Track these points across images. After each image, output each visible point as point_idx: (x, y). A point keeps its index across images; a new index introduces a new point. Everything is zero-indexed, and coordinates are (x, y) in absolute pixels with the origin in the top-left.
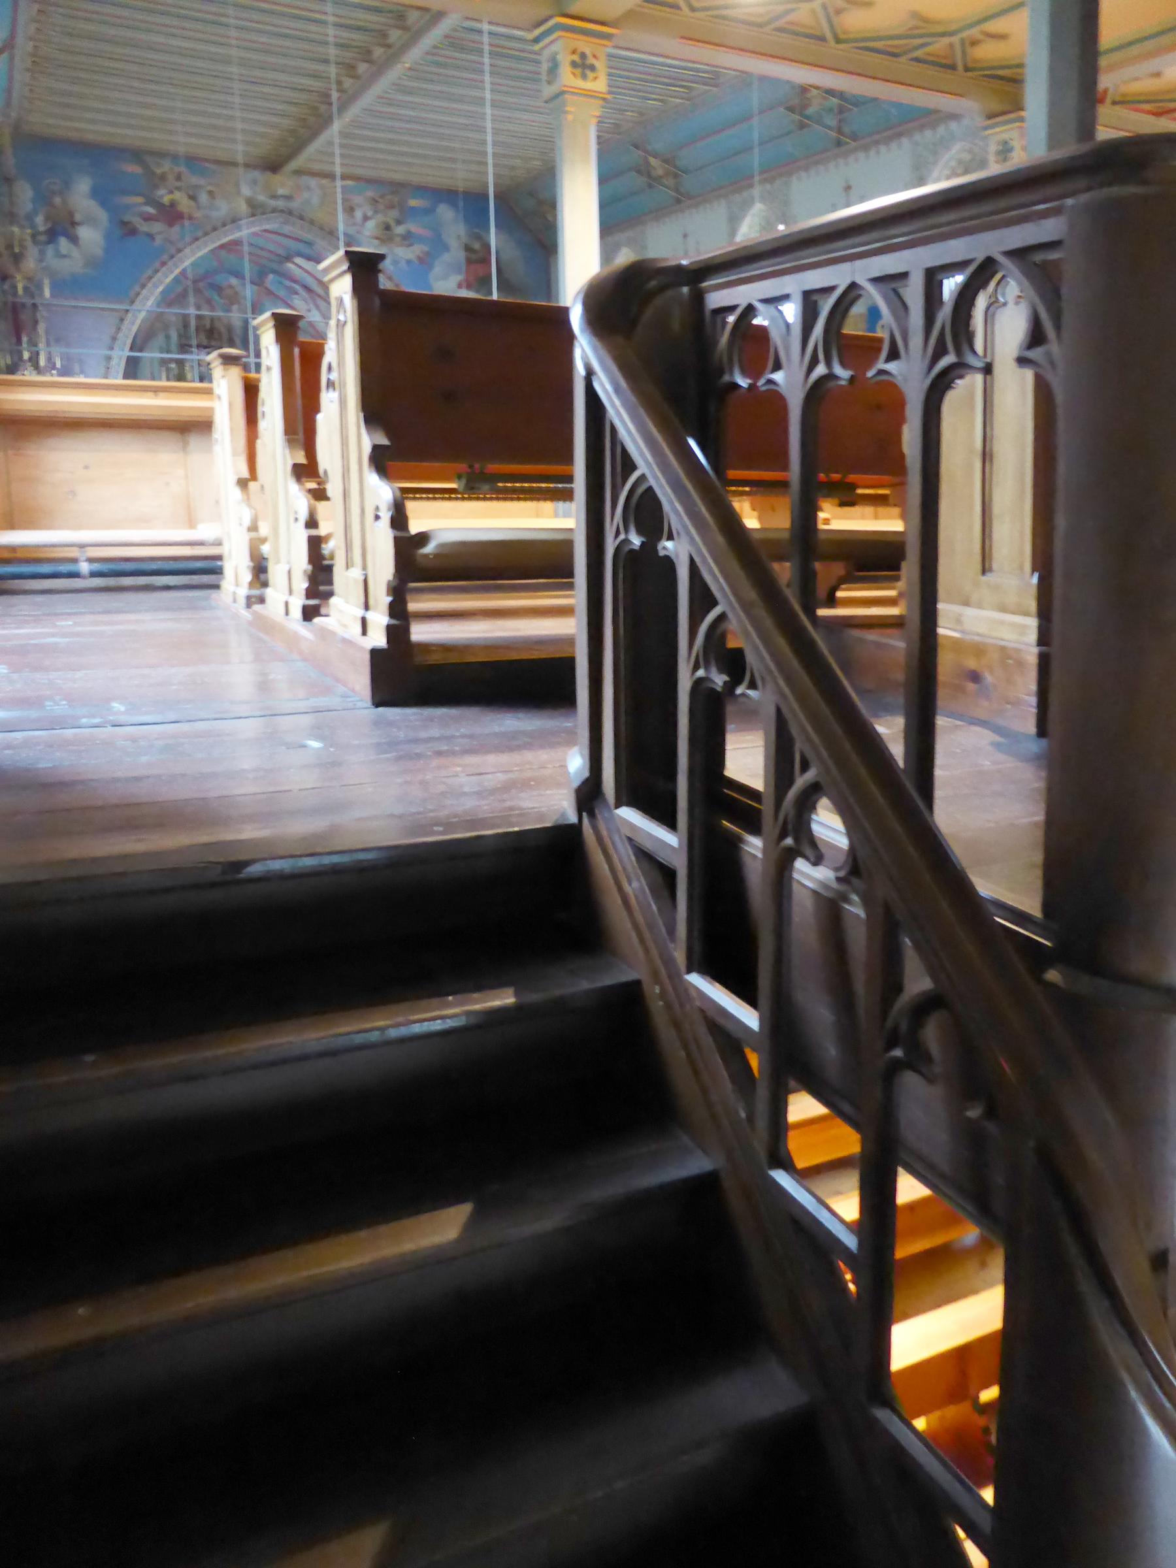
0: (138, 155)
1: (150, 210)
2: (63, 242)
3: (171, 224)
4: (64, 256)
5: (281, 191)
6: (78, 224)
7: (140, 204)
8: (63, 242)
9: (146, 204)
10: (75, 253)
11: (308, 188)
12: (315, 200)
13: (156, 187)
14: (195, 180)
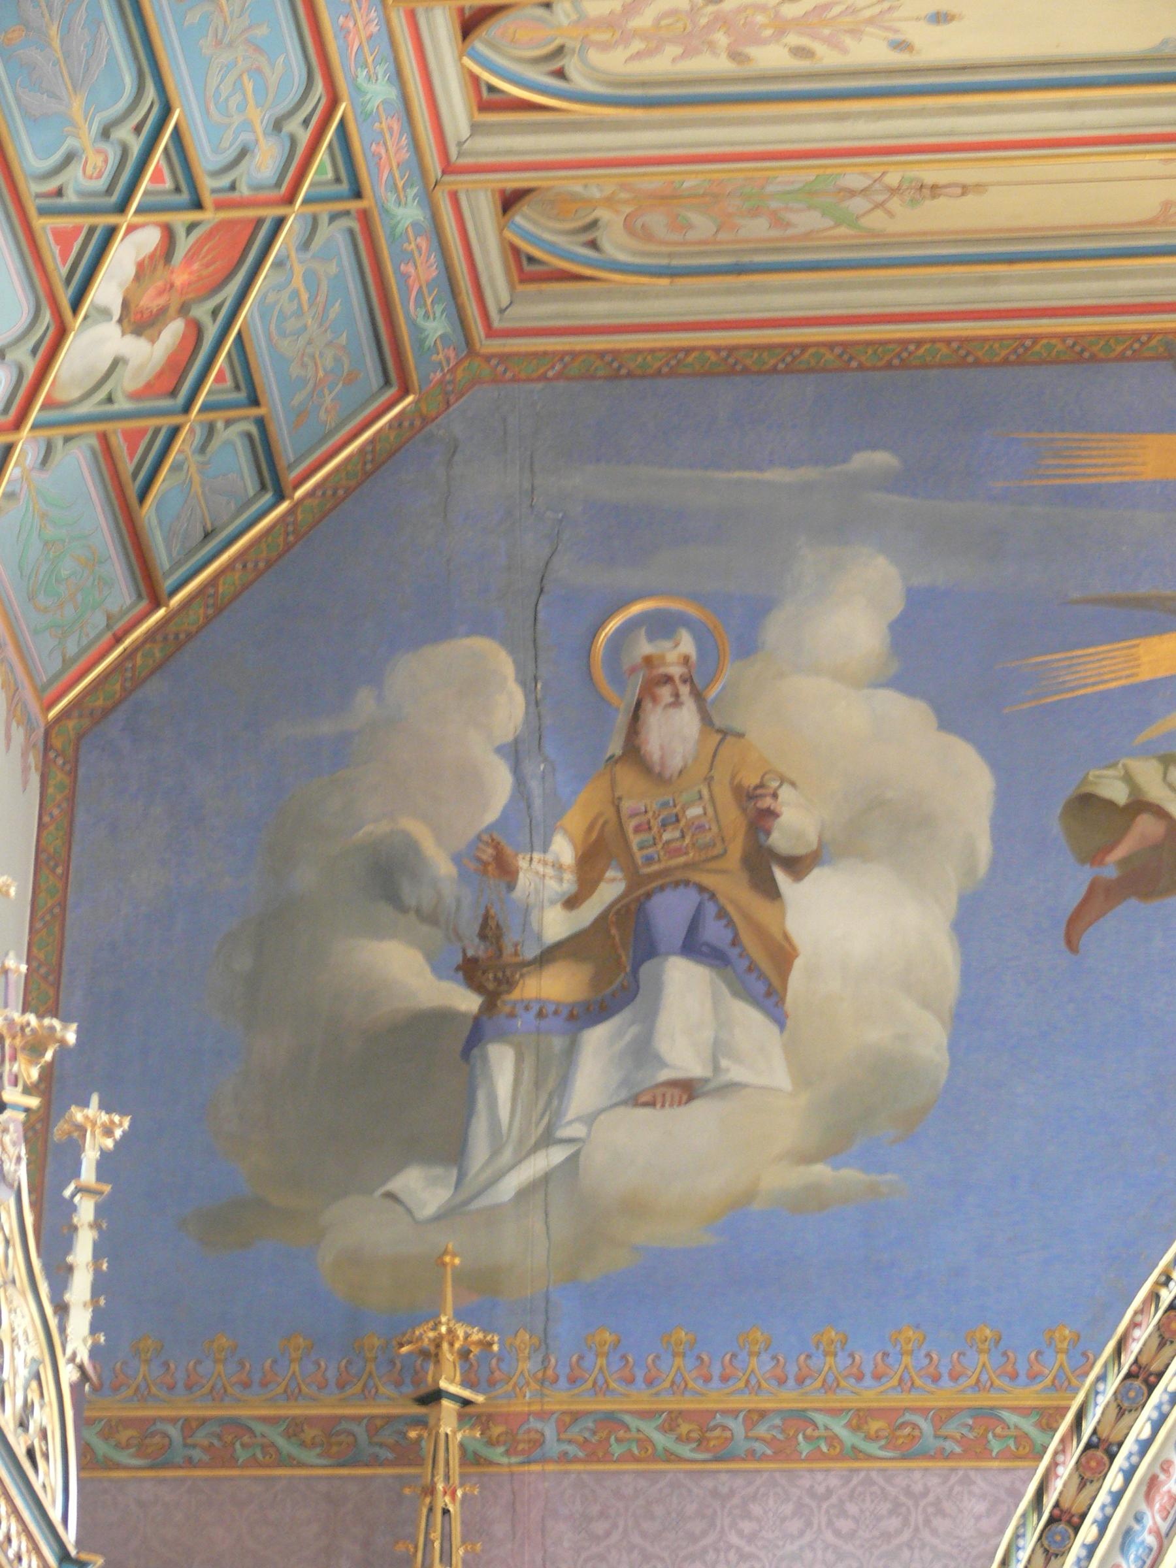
6: (797, 866)
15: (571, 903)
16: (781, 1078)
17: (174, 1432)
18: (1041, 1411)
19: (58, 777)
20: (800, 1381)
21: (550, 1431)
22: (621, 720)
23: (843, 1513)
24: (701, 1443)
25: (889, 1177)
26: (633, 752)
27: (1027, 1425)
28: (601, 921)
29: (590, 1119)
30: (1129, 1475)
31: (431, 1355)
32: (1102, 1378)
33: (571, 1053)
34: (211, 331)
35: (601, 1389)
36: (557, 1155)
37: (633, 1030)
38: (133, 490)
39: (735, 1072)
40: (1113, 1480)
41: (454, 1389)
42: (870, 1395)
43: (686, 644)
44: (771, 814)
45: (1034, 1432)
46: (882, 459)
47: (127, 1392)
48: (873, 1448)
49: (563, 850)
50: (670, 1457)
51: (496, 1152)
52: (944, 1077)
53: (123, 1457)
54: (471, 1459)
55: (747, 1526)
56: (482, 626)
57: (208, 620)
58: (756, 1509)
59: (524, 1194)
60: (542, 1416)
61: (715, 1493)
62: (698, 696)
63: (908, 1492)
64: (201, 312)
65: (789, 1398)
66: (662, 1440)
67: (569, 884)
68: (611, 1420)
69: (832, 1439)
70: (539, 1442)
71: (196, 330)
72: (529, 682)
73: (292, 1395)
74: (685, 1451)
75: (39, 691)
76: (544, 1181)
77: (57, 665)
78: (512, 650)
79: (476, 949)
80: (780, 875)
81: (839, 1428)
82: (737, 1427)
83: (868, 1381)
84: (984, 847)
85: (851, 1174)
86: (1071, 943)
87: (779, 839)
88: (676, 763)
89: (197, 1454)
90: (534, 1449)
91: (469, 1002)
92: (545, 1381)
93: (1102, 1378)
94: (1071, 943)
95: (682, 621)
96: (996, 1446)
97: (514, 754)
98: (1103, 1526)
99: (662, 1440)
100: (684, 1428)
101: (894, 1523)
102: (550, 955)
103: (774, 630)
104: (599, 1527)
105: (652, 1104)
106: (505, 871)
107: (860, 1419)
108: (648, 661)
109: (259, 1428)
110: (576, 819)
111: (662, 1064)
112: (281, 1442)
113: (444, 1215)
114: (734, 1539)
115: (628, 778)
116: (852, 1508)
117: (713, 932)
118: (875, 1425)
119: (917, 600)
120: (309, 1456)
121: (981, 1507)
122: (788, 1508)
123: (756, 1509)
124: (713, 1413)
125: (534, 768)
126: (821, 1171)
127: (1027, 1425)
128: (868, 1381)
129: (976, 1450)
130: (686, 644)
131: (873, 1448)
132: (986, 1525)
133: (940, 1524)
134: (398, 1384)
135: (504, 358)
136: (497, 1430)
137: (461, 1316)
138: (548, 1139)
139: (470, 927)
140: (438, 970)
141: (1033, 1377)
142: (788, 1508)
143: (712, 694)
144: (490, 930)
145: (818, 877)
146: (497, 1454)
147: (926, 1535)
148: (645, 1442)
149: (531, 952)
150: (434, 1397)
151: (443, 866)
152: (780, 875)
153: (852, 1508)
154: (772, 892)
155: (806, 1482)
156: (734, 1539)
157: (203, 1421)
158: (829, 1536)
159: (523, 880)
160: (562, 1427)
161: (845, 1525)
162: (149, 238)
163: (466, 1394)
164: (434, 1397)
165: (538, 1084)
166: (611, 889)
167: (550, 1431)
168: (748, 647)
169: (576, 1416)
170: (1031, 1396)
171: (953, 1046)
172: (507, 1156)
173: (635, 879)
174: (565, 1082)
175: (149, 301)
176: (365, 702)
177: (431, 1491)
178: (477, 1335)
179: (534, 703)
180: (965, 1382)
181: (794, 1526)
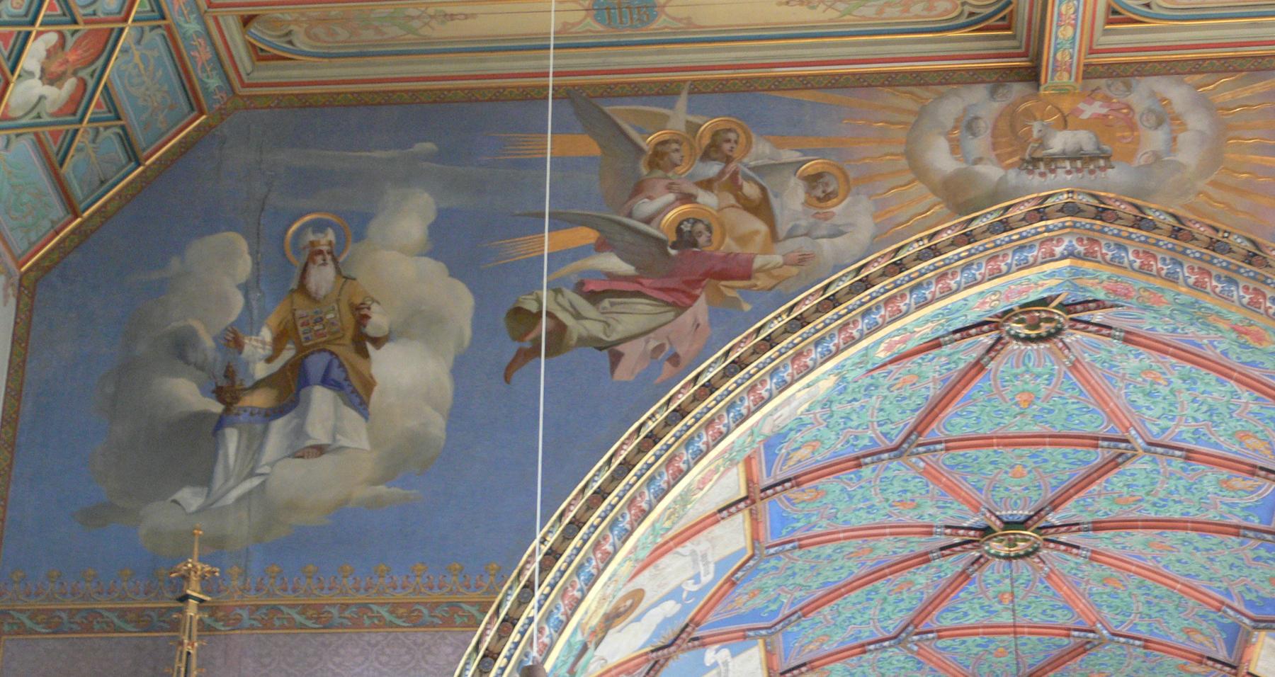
1: (613, 263)
2: (321, 400)
3: (679, 299)
4: (320, 450)
5: (1060, 141)
6: (378, 342)
7: (580, 253)
8: (321, 400)
9: (602, 246)
10: (356, 434)
11: (1164, 117)
12: (1189, 155)
13: (638, 189)
14: (762, 150)
15: (269, 360)
16: (365, 445)
17: (64, 615)
18: (480, 603)
19: (25, 299)
20: (366, 590)
21: (245, 614)
22: (298, 272)
23: (383, 654)
24: (318, 619)
25: (414, 491)
26: (302, 288)
27: (474, 610)
28: (283, 370)
29: (272, 464)
30: (523, 634)
31: (185, 578)
32: (510, 588)
33: (265, 431)
34: (91, 83)
35: (271, 594)
36: (255, 482)
37: (295, 422)
38: (55, 160)
39: (343, 441)
40: (515, 636)
41: (195, 594)
42: (400, 596)
43: (331, 235)
44: (367, 317)
45: (477, 614)
46: (429, 146)
47: (43, 597)
48: (399, 622)
49: (267, 334)
50: (303, 627)
51: (226, 480)
52: (442, 443)
53: (39, 629)
54: (204, 627)
55: (337, 660)
56: (232, 227)
57: (102, 223)
58: (342, 651)
59: (240, 500)
60: (241, 607)
61: (323, 644)
62: (335, 260)
63: (415, 644)
64: (84, 74)
65: (361, 598)
66: (299, 618)
67: (268, 351)
68: (275, 609)
69: (381, 618)
70: (239, 620)
71: (83, 83)
72: (254, 253)
73: (123, 598)
74: (309, 623)
75: (15, 258)
76: (249, 493)
77: (25, 245)
78: (247, 238)
79: (223, 382)
80: (370, 347)
81: (384, 612)
82: (335, 611)
83: (399, 590)
84: (468, 333)
85: (396, 491)
86: (507, 378)
87: (370, 330)
88: (322, 292)
89: (74, 626)
90: (237, 623)
91: (218, 408)
92: (244, 590)
93: (510, 588)
94: (507, 378)
95: (328, 224)
96: (458, 621)
97: (245, 288)
98: (509, 658)
99: (299, 618)
100: (310, 613)
101: (407, 658)
102: (257, 385)
103: (373, 228)
104: (267, 661)
105: (302, 457)
106: (238, 345)
107: (393, 608)
108: (312, 243)
109: (106, 614)
110: (273, 320)
111: (308, 437)
112: (116, 620)
113: (200, 510)
114: (331, 666)
115: (299, 300)
116: (388, 651)
117: (336, 374)
118: (310, 613)
119: (441, 214)
120: (129, 627)
121: (449, 650)
122: (404, 650)
123: (342, 651)
124: (323, 605)
125: (255, 295)
126: (382, 489)
127: (474, 610)
128: (399, 590)
129: (448, 622)
130: (331, 235)
131: (399, 622)
132: (451, 658)
133: (430, 658)
134: (173, 592)
135: (249, 97)
136: (220, 614)
137: (200, 560)
138: (252, 474)
139: (219, 370)
140: (204, 392)
141: (478, 587)
142: (357, 651)
143: (341, 260)
144: (229, 373)
145: (388, 348)
146: (219, 625)
147: (423, 664)
148: (291, 620)
149: (248, 384)
150: (185, 598)
151: (208, 342)
152: (370, 347)
153: (388, 651)
154: (365, 354)
155: (366, 638)
156: (331, 666)
157: (79, 610)
158: (376, 664)
159: (247, 349)
160: (252, 612)
161: (384, 659)
162: (51, 38)
163: (201, 596)
164: (185, 598)
165: (248, 447)
166: (288, 353)
167: (245, 614)
168: (360, 237)
169: (258, 607)
170: (476, 596)
171: (448, 428)
172: (231, 482)
173: (300, 348)
174: (261, 446)
175: (55, 68)
176: (175, 263)
177: (181, 643)
178: (207, 568)
179: (256, 264)
180: (445, 590)
181: (361, 659)
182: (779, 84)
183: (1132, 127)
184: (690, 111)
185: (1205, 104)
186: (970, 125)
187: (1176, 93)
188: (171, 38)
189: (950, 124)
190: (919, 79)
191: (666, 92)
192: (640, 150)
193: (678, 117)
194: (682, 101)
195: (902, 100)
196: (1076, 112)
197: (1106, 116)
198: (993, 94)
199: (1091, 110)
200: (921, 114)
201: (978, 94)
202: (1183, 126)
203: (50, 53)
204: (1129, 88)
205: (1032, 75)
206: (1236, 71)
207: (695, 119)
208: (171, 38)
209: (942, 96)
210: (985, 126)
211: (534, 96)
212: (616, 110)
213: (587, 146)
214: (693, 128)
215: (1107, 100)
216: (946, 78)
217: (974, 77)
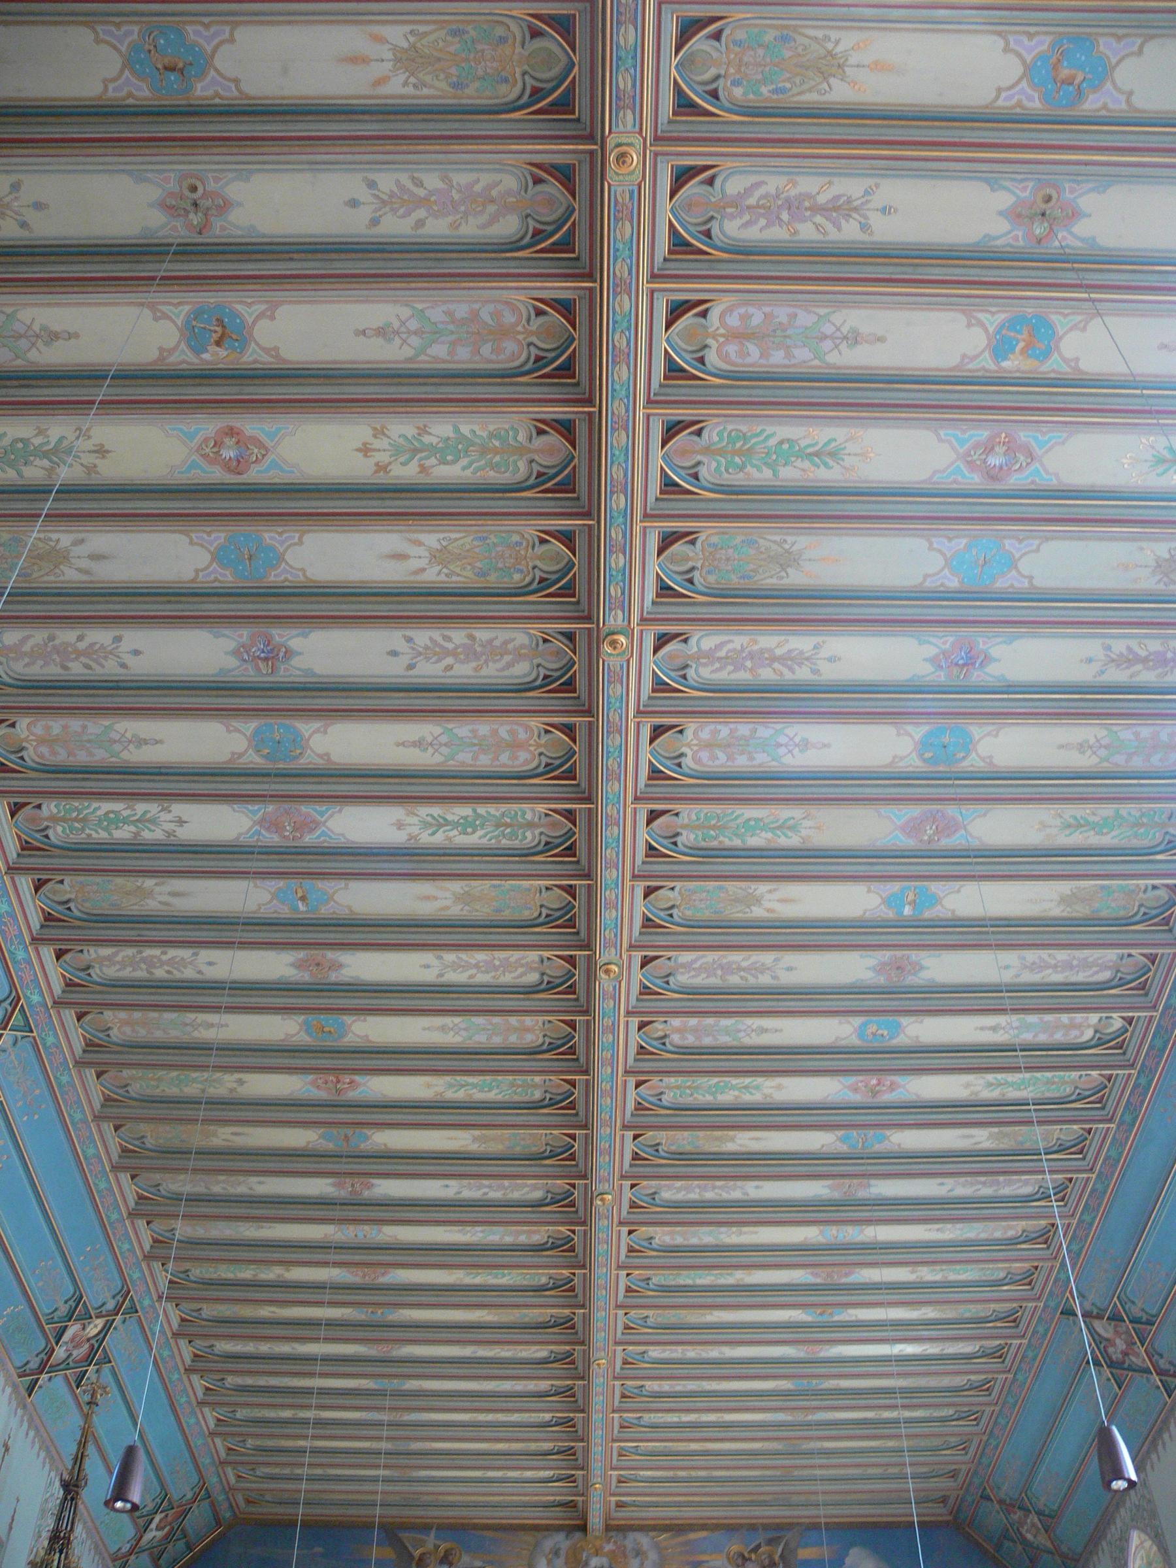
0: (392, 1532)
11: (638, 1553)
162: (163, 1515)
175: (162, 1525)
182: (475, 1527)
183: (625, 1556)
184: (436, 1537)
185: (657, 1546)
186: (556, 1553)
187: (644, 1540)
188: (212, 1504)
189: (547, 1550)
190: (536, 1528)
191: (426, 1528)
192: (411, 1556)
193: (431, 1540)
194: (433, 1533)
195: (528, 1538)
196: (602, 1548)
197: (614, 1551)
198: (567, 1536)
199: (608, 1547)
200: (537, 1545)
201: (560, 1537)
202: (647, 1558)
203: (161, 1521)
204: (625, 1538)
205: (583, 1528)
206: (671, 1530)
207: (438, 1542)
208: (212, 1504)
209: (545, 1537)
210: (563, 1553)
211: (368, 1526)
212: (405, 1536)
213: (389, 1553)
214: (437, 1547)
215: (615, 1542)
216: (548, 1528)
217: (559, 1528)
